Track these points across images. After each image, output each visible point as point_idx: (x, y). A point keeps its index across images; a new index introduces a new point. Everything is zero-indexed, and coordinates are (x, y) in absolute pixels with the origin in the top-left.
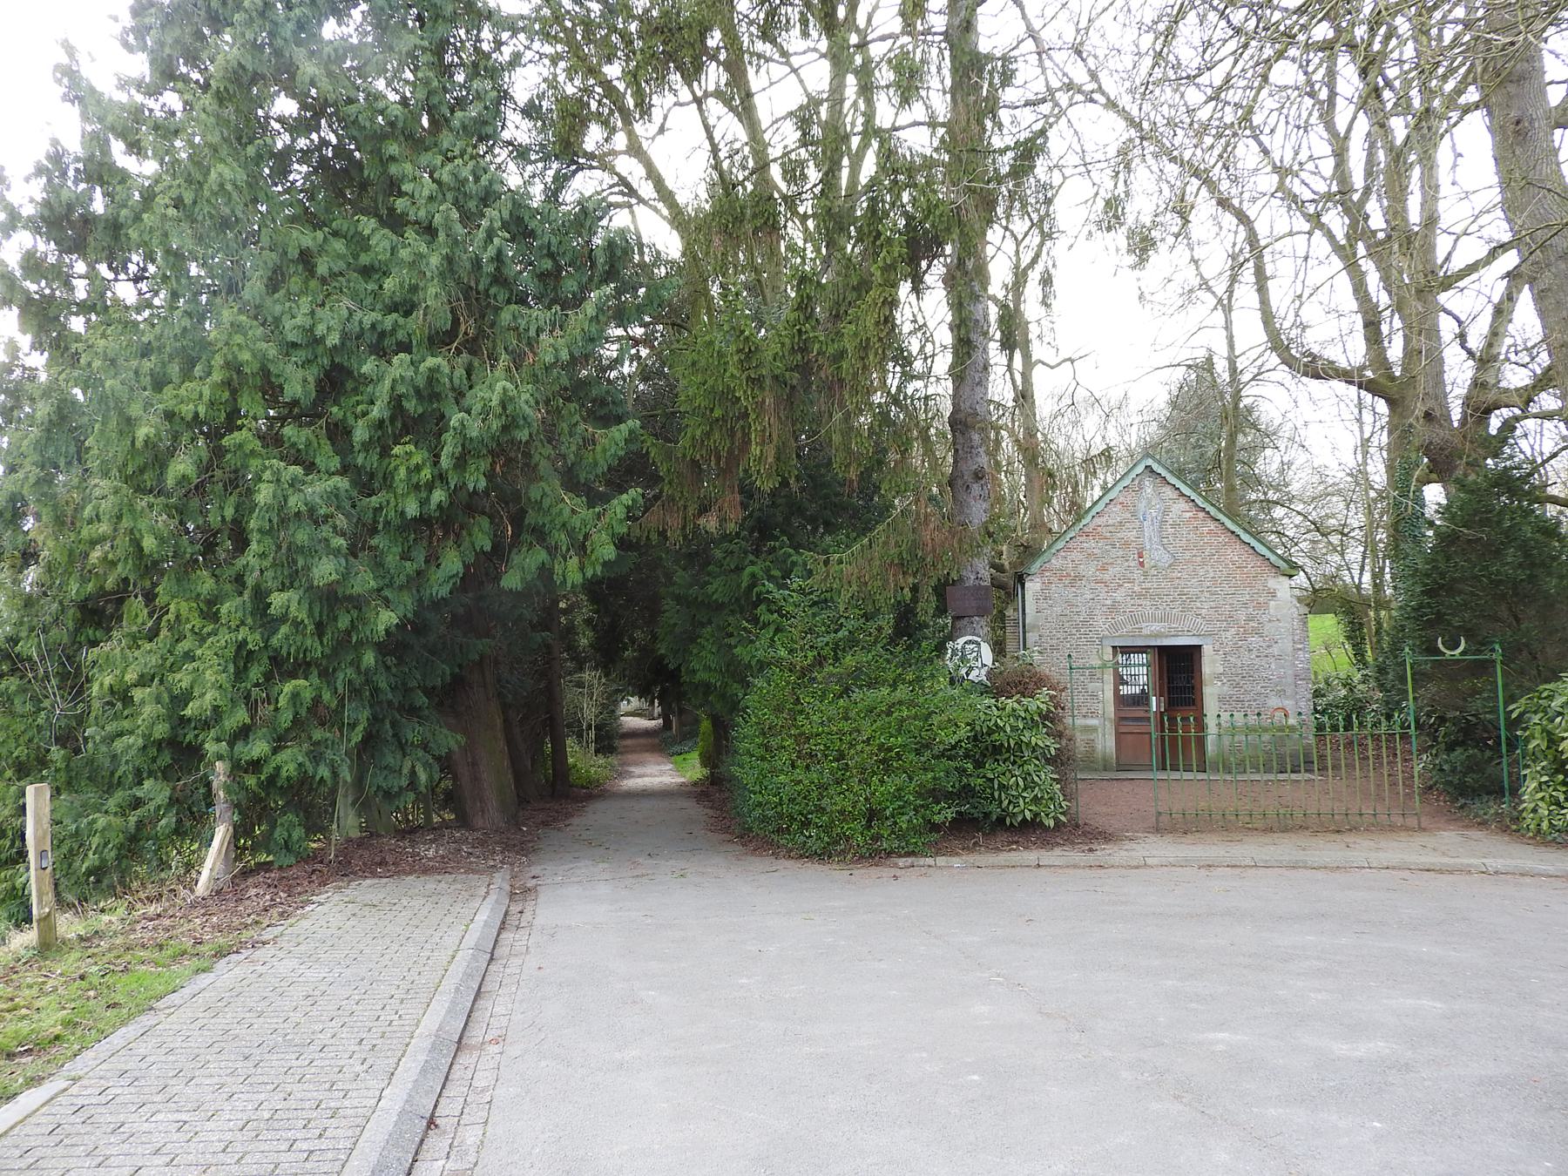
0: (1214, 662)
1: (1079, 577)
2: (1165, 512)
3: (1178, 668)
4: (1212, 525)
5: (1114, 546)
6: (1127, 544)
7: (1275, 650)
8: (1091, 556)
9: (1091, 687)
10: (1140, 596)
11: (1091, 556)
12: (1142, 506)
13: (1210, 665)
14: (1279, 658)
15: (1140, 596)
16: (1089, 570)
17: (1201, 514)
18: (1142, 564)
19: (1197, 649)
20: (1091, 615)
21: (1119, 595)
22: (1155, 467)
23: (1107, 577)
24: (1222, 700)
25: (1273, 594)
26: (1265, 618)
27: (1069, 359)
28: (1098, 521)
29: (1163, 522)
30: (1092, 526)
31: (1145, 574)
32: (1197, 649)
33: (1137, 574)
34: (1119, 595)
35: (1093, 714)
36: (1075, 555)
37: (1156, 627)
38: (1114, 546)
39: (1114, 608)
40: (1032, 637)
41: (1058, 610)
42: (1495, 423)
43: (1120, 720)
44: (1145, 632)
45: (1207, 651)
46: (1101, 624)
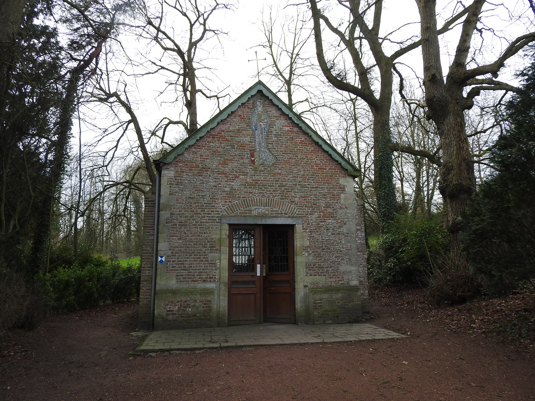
0: (303, 237)
1: (205, 169)
2: (271, 126)
3: (276, 242)
5: (233, 147)
6: (242, 146)
7: (344, 229)
8: (215, 153)
9: (211, 256)
10: (251, 185)
11: (215, 153)
12: (254, 119)
13: (300, 240)
14: (347, 235)
15: (251, 185)
16: (214, 163)
17: (296, 129)
18: (253, 162)
19: (291, 227)
20: (213, 198)
21: (236, 184)
22: (265, 91)
24: (308, 266)
25: (343, 189)
26: (337, 206)
27: (216, 96)
28: (222, 127)
29: (269, 132)
30: (217, 130)
31: (255, 169)
32: (291, 227)
33: (249, 169)
35: (212, 279)
36: (203, 151)
37: (262, 210)
38: (233, 147)
39: (231, 194)
40: (165, 215)
41: (187, 193)
42: (467, 90)
43: (232, 283)
44: (254, 213)
45: (299, 228)
46: (221, 206)
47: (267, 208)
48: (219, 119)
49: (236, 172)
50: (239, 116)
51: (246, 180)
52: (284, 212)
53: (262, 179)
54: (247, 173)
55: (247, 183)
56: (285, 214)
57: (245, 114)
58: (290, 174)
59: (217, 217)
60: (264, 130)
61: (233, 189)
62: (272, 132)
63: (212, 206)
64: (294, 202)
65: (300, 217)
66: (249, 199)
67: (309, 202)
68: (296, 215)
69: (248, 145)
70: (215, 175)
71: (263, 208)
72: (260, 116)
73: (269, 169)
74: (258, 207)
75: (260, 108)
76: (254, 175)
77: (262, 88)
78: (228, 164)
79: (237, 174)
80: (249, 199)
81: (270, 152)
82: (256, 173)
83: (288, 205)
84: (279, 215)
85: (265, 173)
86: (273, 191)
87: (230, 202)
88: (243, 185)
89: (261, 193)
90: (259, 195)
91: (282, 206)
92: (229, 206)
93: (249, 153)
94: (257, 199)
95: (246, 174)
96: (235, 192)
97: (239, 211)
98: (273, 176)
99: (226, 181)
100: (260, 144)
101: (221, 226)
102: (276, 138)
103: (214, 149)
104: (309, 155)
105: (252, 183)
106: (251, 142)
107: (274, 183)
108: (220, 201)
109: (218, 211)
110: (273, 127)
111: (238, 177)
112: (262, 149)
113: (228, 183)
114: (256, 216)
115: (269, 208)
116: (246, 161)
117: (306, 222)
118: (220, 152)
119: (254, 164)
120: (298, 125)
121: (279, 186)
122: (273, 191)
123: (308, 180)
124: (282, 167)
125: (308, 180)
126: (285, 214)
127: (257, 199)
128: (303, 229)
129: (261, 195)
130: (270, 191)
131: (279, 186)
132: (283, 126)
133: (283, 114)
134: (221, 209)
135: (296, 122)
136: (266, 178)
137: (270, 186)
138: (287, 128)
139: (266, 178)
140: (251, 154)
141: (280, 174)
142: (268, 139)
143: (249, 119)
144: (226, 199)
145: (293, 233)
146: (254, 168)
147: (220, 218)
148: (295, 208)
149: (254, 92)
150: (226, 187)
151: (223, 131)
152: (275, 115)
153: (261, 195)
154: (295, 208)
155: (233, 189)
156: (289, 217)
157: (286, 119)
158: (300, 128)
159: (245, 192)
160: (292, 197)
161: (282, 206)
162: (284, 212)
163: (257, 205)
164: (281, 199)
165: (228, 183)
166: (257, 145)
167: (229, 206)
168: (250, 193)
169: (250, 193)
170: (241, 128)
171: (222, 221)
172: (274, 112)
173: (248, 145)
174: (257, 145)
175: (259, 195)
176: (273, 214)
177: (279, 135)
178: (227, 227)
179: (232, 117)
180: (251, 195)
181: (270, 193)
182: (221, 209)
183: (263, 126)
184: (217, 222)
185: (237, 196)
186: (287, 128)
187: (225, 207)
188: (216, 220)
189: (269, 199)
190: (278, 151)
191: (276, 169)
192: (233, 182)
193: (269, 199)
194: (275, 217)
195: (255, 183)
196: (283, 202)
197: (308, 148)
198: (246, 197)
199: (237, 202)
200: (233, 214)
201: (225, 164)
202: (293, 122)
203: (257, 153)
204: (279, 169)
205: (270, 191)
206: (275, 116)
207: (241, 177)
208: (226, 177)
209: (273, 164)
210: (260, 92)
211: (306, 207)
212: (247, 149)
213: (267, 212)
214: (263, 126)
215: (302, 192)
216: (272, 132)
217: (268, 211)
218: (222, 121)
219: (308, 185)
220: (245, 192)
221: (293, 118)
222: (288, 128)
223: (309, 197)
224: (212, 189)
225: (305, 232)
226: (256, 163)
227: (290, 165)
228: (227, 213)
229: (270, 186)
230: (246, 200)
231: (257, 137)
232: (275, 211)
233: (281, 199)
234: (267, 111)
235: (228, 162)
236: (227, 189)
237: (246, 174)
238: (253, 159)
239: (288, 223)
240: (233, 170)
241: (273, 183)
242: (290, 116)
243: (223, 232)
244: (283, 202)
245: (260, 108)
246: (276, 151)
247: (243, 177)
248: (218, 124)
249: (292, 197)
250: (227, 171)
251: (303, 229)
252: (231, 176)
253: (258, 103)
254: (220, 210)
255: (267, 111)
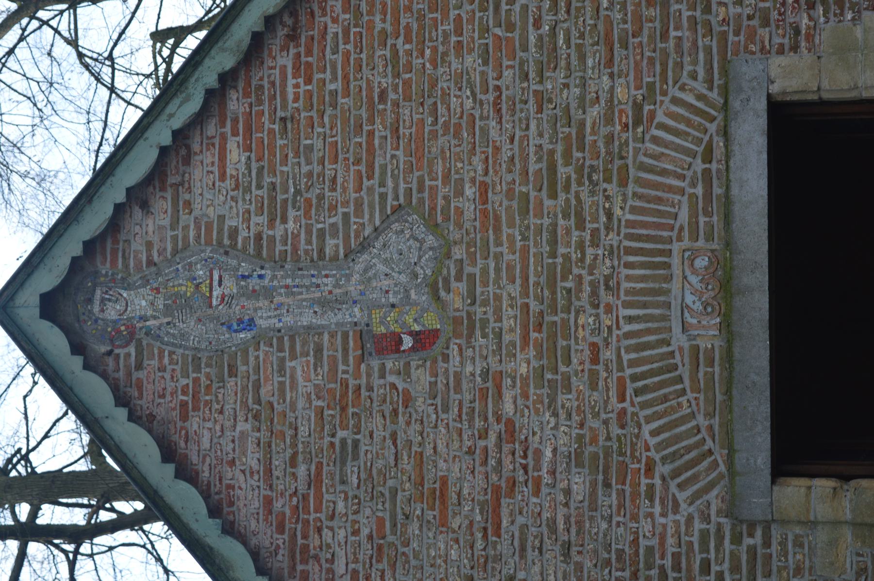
4: (281, 59)
5: (348, 452)
6: (343, 400)
10: (553, 353)
12: (195, 330)
15: (553, 353)
17: (236, 103)
18: (425, 340)
21: (551, 437)
22: (47, 280)
23: (473, 486)
29: (260, 250)
30: (265, 535)
31: (466, 327)
33: (465, 363)
34: (551, 437)
37: (689, 290)
39: (608, 465)
44: (709, 335)
45: (794, 76)
46: (674, 519)
47: (675, 261)
48: (208, 529)
49: (484, 434)
50: (185, 417)
51: (525, 380)
52: (699, 166)
53: (515, 289)
54: (485, 374)
55: (540, 373)
56: (708, 157)
57: (170, 386)
58: (485, 131)
59: (737, 539)
60: (253, 283)
61: (579, 454)
62: (259, 237)
63: (677, 567)
64: (638, 107)
65: (725, 72)
66: (632, 363)
67: (639, 20)
68: (714, 95)
69: (333, 369)
70: (504, 547)
71: (675, 286)
72: (178, 305)
73: (458, 252)
74: (675, 312)
75: (140, 302)
76: (499, 335)
77: (28, 304)
78: (444, 481)
79: (496, 428)
80: (632, 363)
81: (365, 246)
82: (485, 323)
83: (655, 140)
84: (717, 190)
85: (485, 271)
86: (581, 225)
87: (650, 470)
88: (553, 400)
89: (594, 293)
90: (609, 309)
91: (664, 172)
92: (676, 474)
93: (375, 363)
94: (630, 319)
95: (494, 383)
96: (594, 440)
97: (701, 420)
98: (497, 230)
99: (537, 493)
100: (325, 304)
101: (784, 522)
102: (291, 213)
103: (367, 550)
104: (371, 26)
105: (539, 346)
106: (319, 350)
107: (533, 221)
108: (646, 526)
109: (704, 536)
110: (234, 233)
111: (510, 423)
112: (353, 288)
113: (547, 479)
114: (727, 327)
115: (676, 247)
116: (422, 377)
117: (752, 36)
118: (381, 522)
119: (434, 334)
120: (210, 93)
121: (553, 195)
122: (581, 225)
123: (511, 27)
124: (447, 177)
125: (511, 27)
126: (708, 157)
127: (630, 319)
128: (795, 48)
129: (605, 297)
130: (581, 246)
131: (553, 195)
132: (223, 177)
133: (157, 175)
134: (690, 519)
135: (194, 105)
136: (510, 268)
137: (553, 242)
138: (235, 155)
139: (510, 268)
140: (381, 351)
141: (484, 189)
142: (297, 259)
143: (196, 360)
144: (635, 495)
145: (822, 103)
146: (457, 335)
147: (743, 525)
148: (675, 101)
149: (54, 340)
150: (568, 492)
151: (268, 502)
152: (166, 222)
153: (605, 297)
154: (675, 101)
155: (579, 454)
156: (725, 132)
157: (187, 161)
158: (227, 79)
159: (594, 386)
160: (609, 120)
161: (664, 172)
162: (699, 166)
163: (665, 318)
164: (623, 183)
165: (547, 479)
166: (331, 319)
167: (676, 474)
168: (595, 360)
169: (595, 360)
170: (244, 403)
171: (758, 514)
172: (150, 229)
173: (333, 369)
174: (331, 319)
175: (609, 309)
176: (710, 226)
177: (273, 199)
178: (793, 490)
179: (194, 459)
180: (607, 354)
181: (595, 244)
182: (690, 519)
183: (230, 286)
184: (767, 544)
185: (616, 431)
186: (235, 155)
187: (682, 496)
188: (752, 551)
189: (629, 251)
190: (359, 204)
191: (460, 212)
192: (538, 453)
193: (629, 251)
194: (727, 219)
195: (539, 327)
196: (642, 167)
197: (332, 28)
198: (621, 381)
199: (646, 429)
200: (720, 455)
201: (440, 495)
202: (199, 119)
203: (376, 315)
204: (460, 193)
205: (581, 246)
206: (174, 225)
207: (508, 408)
208: (511, 493)
209: (433, 227)
210: (50, 306)
211: (665, 36)
212: (357, 375)
213: (701, 262)
214: (230, 286)
215: (582, 58)
216: (259, 237)
217: (695, 253)
218: (214, 511)
219: (537, 24)
220: (594, 386)
221: (177, 123)
222: (232, 145)
223: (609, 21)
224: (579, 567)
225: (809, 37)
226: (432, 321)
227: (434, 135)
228: (711, 486)
229: (553, 242)
230: (635, 378)
231: (288, 319)
232: (694, 215)
233: (623, 183)
234: (150, 263)
235: (429, 477)
236: (579, 484)
237: (494, 383)
238: (408, 342)
239: (761, 142)
240: (471, 452)
241: (539, 230)
242: (166, 139)
243: (821, 510)
244: (642, 167)
245: (140, 302)
246: (359, 212)
247: (508, 396)
248: (230, 529)
249: (609, 120)
250: (479, 477)
251: (795, 48)
252: (507, 461)
253: (112, 313)
254: (698, 525)
255: (150, 263)
